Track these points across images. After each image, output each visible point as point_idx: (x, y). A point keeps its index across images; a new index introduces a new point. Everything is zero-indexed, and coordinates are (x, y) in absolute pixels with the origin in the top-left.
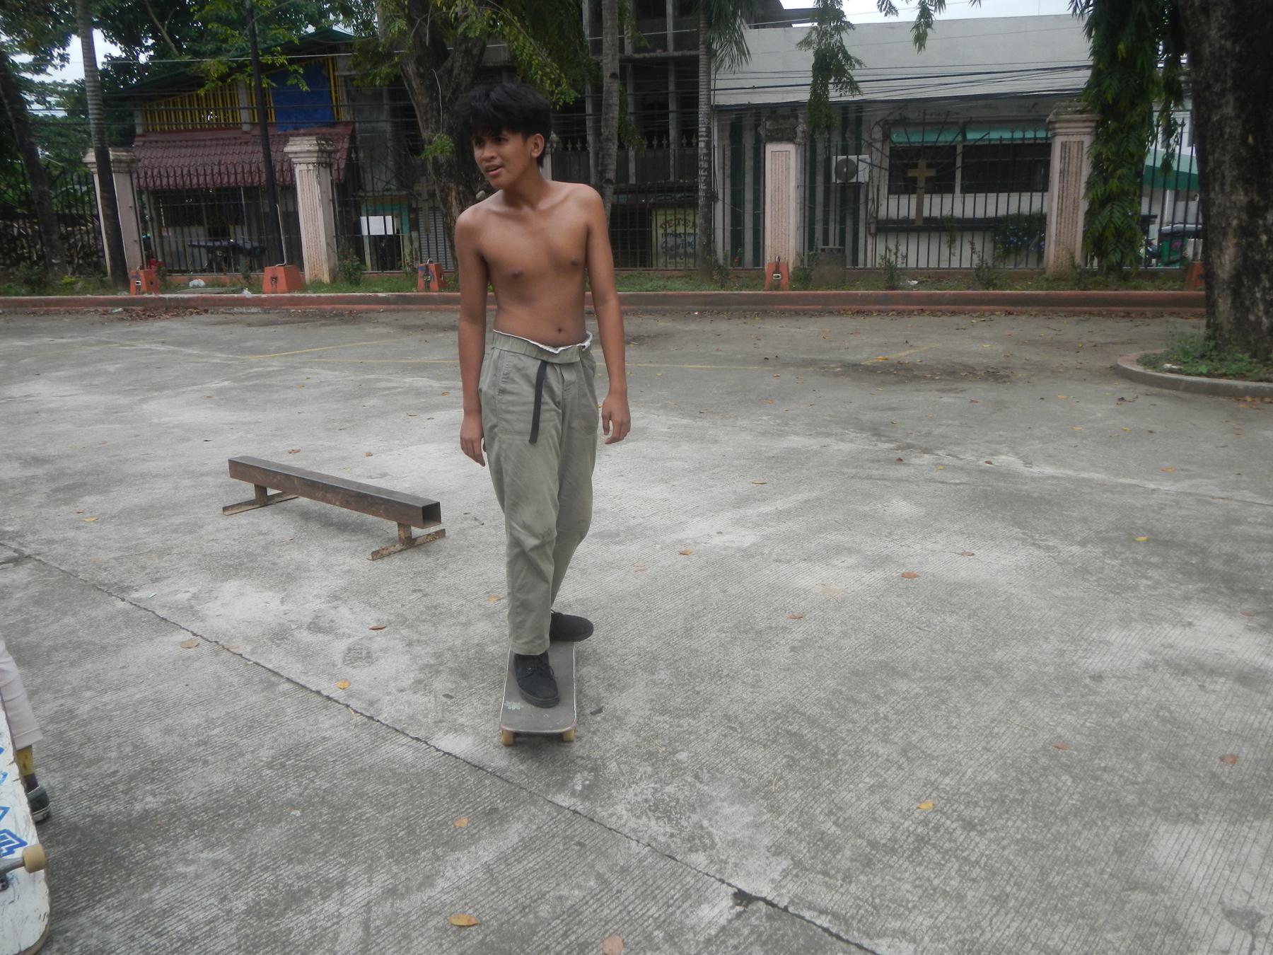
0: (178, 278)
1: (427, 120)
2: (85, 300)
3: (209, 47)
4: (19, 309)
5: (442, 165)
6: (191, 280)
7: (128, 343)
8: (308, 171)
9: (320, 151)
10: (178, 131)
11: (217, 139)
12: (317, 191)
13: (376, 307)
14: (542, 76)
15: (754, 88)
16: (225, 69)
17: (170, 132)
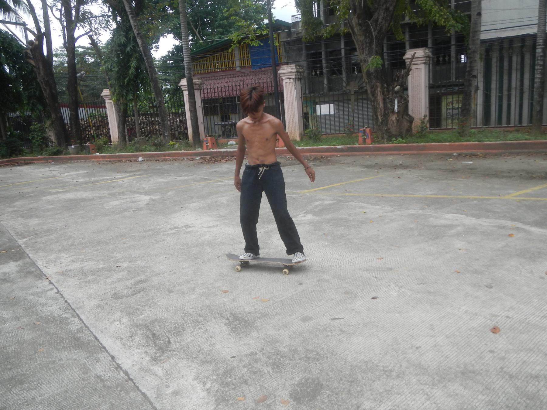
0: (222, 141)
1: (363, 49)
2: (184, 152)
3: (216, 37)
4: (151, 159)
5: (372, 73)
6: (228, 141)
7: (218, 179)
8: (290, 82)
9: (297, 72)
10: (208, 73)
11: (225, 75)
12: (294, 92)
13: (335, 153)
14: (439, 17)
15: (501, 29)
16: (240, 38)
17: (205, 73)
